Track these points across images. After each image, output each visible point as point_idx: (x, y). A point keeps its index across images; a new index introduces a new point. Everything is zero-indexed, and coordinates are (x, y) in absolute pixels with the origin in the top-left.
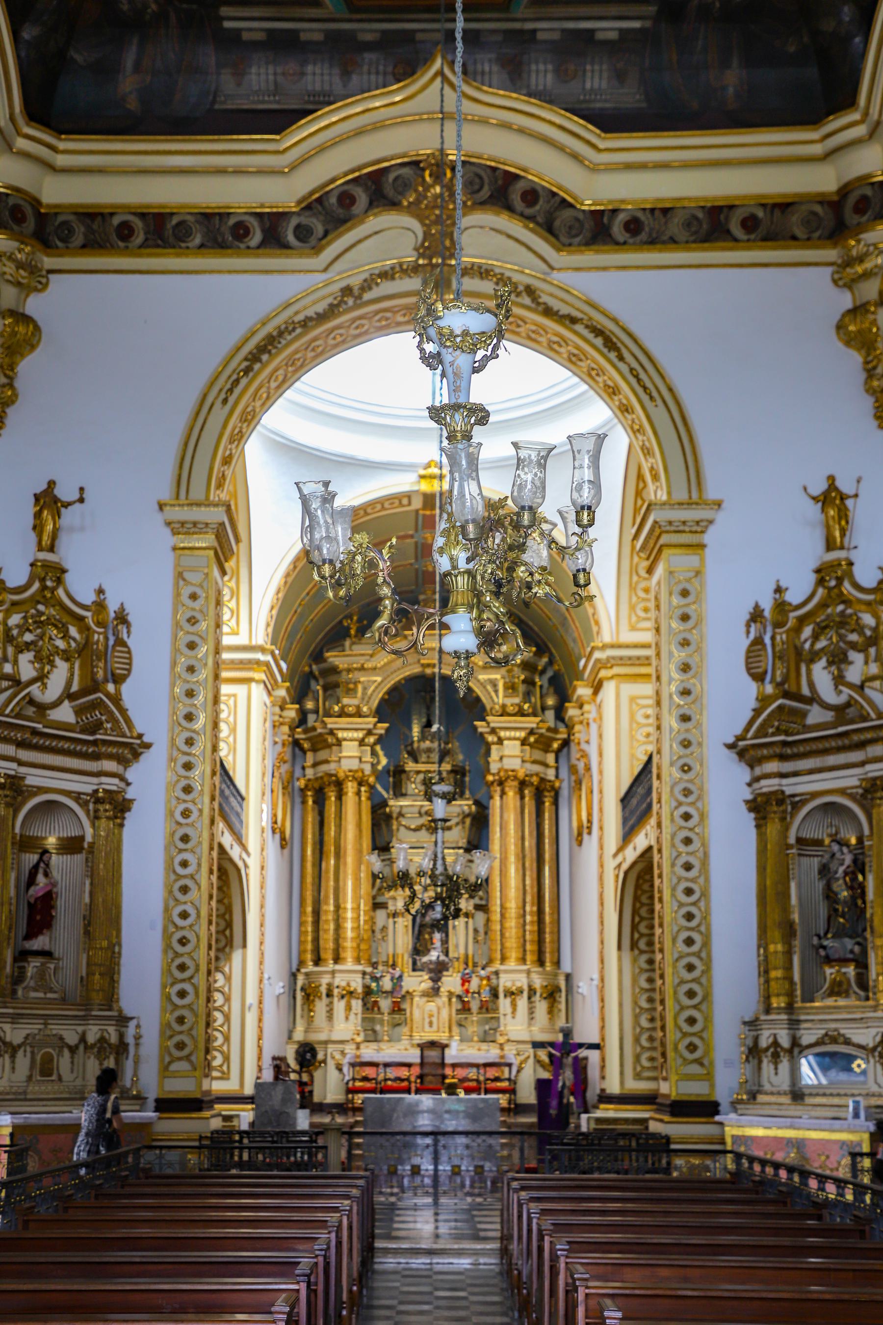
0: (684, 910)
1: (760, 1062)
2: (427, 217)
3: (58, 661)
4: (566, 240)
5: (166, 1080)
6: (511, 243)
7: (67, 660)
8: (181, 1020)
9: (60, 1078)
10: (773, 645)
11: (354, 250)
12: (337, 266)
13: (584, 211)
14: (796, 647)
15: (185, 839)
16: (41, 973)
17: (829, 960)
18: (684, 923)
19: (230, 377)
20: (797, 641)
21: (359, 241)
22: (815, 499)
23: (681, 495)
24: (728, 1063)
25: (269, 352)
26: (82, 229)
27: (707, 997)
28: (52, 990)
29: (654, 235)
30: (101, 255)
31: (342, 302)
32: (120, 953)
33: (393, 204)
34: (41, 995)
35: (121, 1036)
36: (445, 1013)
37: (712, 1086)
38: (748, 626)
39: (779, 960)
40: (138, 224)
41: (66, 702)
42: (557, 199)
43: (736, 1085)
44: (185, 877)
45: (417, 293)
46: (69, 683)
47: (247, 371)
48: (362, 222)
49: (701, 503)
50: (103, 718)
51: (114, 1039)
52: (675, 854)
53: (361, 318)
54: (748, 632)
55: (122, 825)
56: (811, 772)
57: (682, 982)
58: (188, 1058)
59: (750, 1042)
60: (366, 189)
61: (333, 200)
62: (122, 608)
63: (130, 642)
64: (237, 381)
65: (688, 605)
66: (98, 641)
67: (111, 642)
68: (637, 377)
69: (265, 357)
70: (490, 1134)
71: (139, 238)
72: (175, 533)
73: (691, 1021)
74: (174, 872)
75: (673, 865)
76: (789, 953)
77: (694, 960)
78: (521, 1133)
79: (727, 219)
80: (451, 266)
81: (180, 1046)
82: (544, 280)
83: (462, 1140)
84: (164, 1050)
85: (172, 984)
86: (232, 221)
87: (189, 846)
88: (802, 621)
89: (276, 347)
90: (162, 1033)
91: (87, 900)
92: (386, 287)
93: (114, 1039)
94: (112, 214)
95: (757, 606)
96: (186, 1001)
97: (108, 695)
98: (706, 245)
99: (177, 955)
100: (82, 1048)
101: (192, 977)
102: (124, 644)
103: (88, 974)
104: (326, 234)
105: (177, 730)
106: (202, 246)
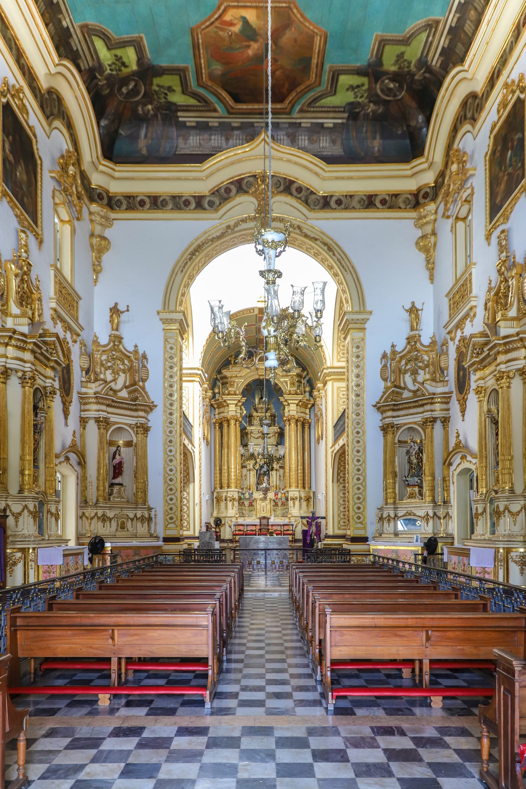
0: (357, 468)
3: (121, 374)
4: (313, 207)
6: (291, 208)
7: (124, 373)
8: (171, 509)
11: (231, 211)
12: (225, 217)
15: (171, 441)
16: (119, 492)
17: (409, 485)
21: (233, 207)
22: (406, 310)
23: (357, 309)
24: (372, 523)
27: (364, 499)
28: (123, 498)
31: (226, 232)
33: (246, 192)
35: (149, 515)
36: (269, 506)
37: (366, 531)
38: (381, 360)
39: (391, 486)
40: (147, 200)
42: (309, 191)
43: (375, 531)
46: (125, 382)
47: (190, 259)
48: (234, 199)
51: (147, 516)
53: (234, 238)
54: (381, 363)
55: (147, 436)
56: (404, 416)
57: (355, 494)
58: (174, 523)
59: (380, 516)
60: (236, 186)
61: (223, 190)
62: (144, 353)
63: (148, 366)
64: (186, 263)
67: (141, 366)
68: (340, 262)
69: (197, 253)
71: (148, 206)
72: (164, 323)
73: (359, 508)
75: (353, 451)
76: (394, 483)
77: (360, 486)
81: (171, 518)
82: (305, 223)
83: (275, 552)
86: (183, 199)
87: (172, 444)
88: (401, 358)
90: (164, 514)
91: (135, 464)
92: (244, 226)
93: (147, 516)
97: (140, 386)
99: (169, 485)
102: (146, 367)
104: (220, 204)
105: (167, 400)
106: (172, 209)
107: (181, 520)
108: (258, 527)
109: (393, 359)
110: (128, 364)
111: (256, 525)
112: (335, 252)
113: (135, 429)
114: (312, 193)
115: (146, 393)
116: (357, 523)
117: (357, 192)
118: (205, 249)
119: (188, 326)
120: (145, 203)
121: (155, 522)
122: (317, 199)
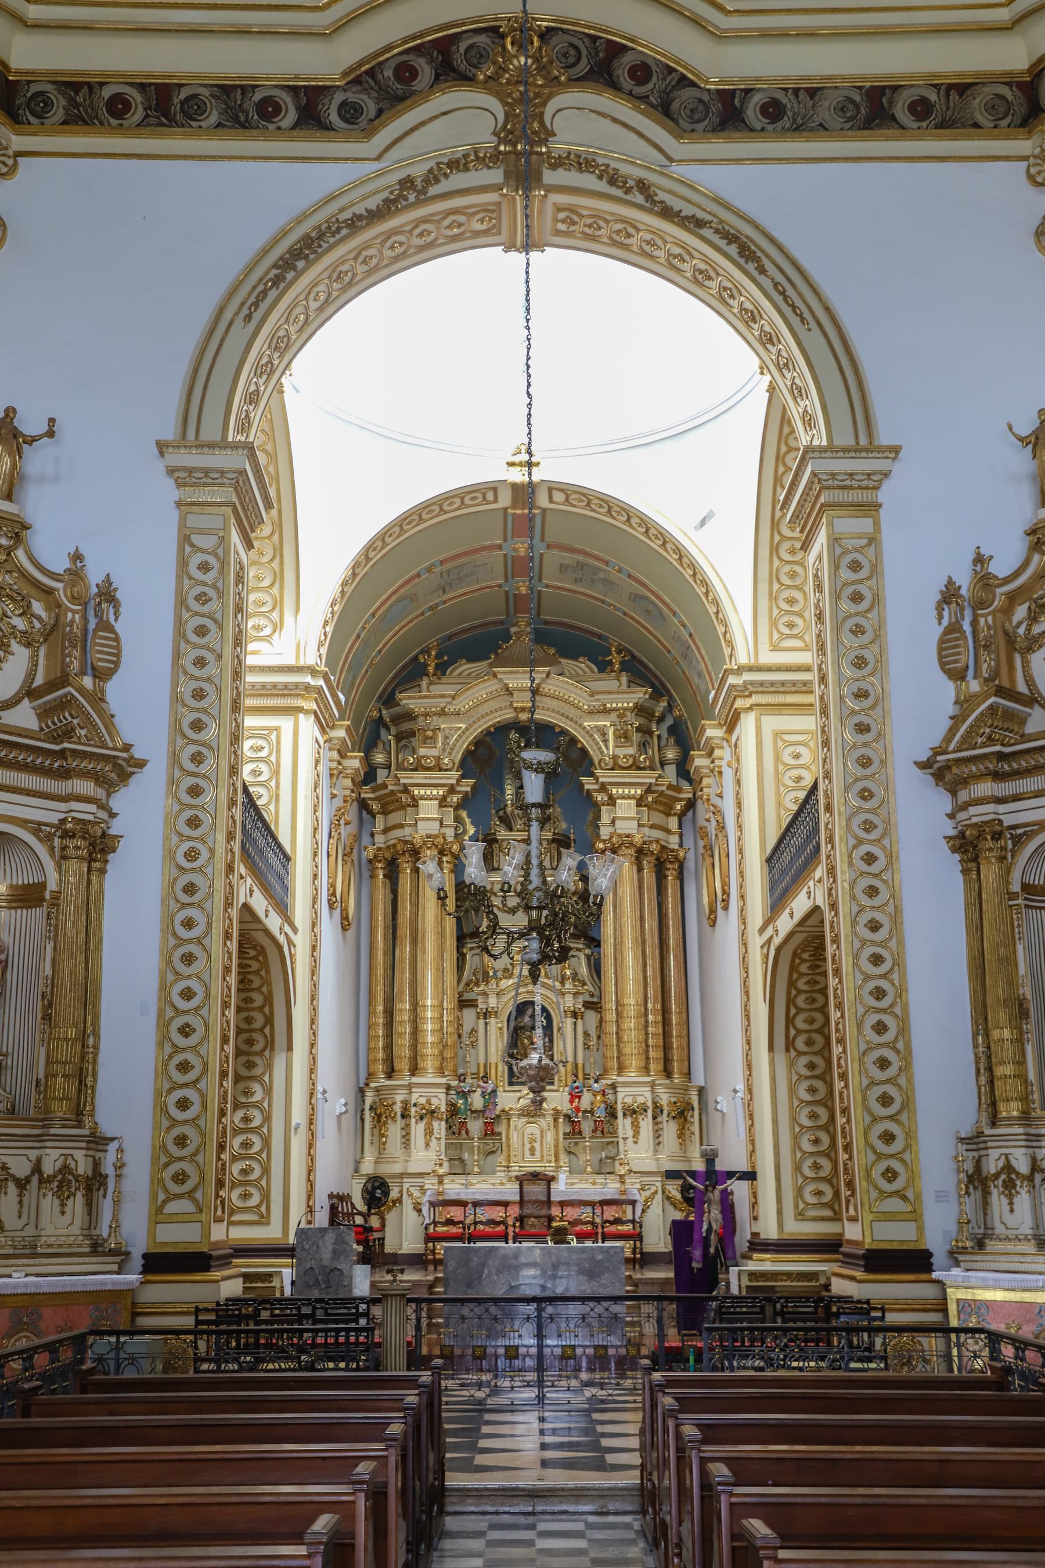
0: (871, 985)
1: (986, 1194)
2: (510, 95)
4: (691, 127)
6: (617, 127)
7: (28, 645)
8: (181, 1141)
10: (975, 632)
11: (416, 133)
12: (395, 153)
13: (709, 90)
14: (1006, 633)
18: (872, 1002)
19: (254, 287)
20: (1007, 624)
21: (423, 124)
23: (845, 439)
25: (306, 257)
26: (63, 102)
29: (799, 121)
30: (86, 134)
32: (96, 1047)
33: (466, 79)
38: (940, 609)
39: (1008, 1051)
40: (136, 97)
41: (26, 701)
43: (953, 1227)
44: (189, 941)
45: (497, 188)
47: (277, 281)
49: (871, 449)
50: (75, 721)
52: (856, 909)
53: (425, 220)
54: (940, 617)
58: (190, 1195)
60: (431, 61)
61: (389, 73)
63: (118, 627)
64: (265, 293)
65: (860, 581)
66: (73, 621)
67: (92, 625)
68: (783, 293)
69: (301, 264)
70: (616, 1299)
71: (137, 114)
74: (175, 934)
75: (854, 923)
76: (1019, 1041)
78: (659, 1299)
79: (891, 102)
80: (541, 154)
82: (662, 173)
83: (574, 1310)
84: (156, 1182)
85: (171, 1090)
86: (258, 96)
87: (195, 899)
88: (1013, 598)
89: (316, 252)
91: (48, 971)
92: (458, 180)
94: (102, 84)
95: (950, 581)
96: (190, 1114)
97: (81, 690)
98: (866, 132)
99: (177, 1049)
100: (35, 1179)
101: (197, 1081)
102: (111, 629)
103: (46, 1077)
104: (380, 112)
105: (180, 742)
106: (219, 125)
107: (220, 1184)
108: (514, 1211)
109: (979, 604)
110: (44, 615)
111: (505, 1204)
112: (765, 261)
113: (57, 842)
114: (684, 82)
115: (101, 712)
116: (883, 1195)
117: (830, 78)
118: (329, 249)
119: (269, 506)
120: (127, 106)
121: (118, 1192)
122: (700, 101)
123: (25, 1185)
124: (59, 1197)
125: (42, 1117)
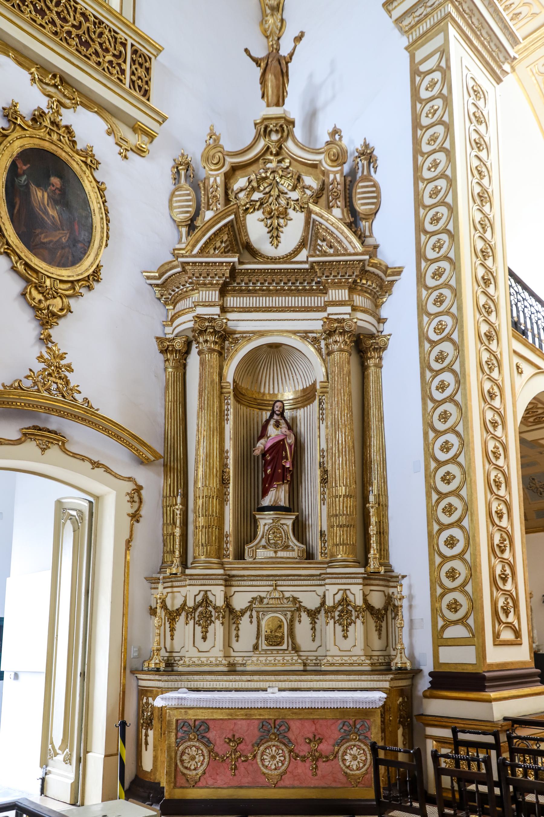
5: (440, 648)
9: (296, 649)
28: (286, 547)
34: (272, 554)
81: (454, 606)
84: (435, 611)
85: (440, 531)
99: (442, 496)
123: (315, 615)
124: (340, 624)
125: (328, 559)
